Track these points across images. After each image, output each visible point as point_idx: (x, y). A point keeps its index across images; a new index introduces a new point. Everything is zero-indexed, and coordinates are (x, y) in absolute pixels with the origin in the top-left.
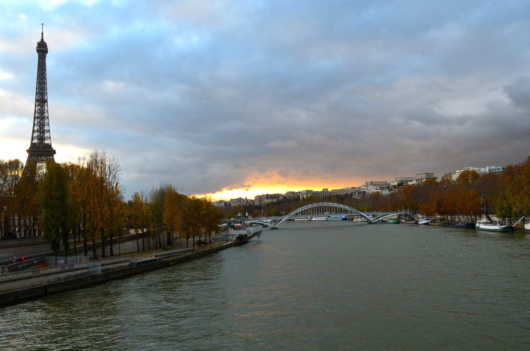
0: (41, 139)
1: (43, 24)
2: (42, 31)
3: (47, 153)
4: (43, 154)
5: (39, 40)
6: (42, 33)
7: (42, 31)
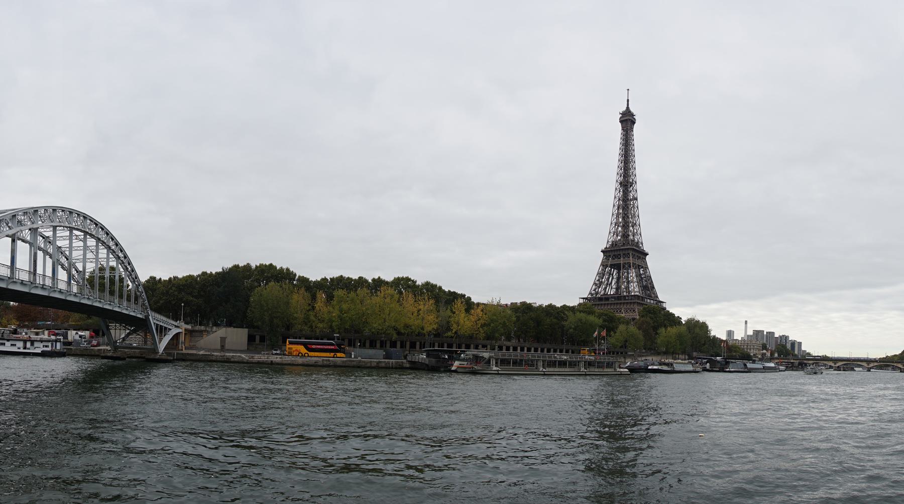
0: (625, 236)
1: (628, 90)
2: (628, 97)
3: (624, 252)
4: (619, 255)
5: (624, 109)
6: (628, 100)
7: (628, 97)
